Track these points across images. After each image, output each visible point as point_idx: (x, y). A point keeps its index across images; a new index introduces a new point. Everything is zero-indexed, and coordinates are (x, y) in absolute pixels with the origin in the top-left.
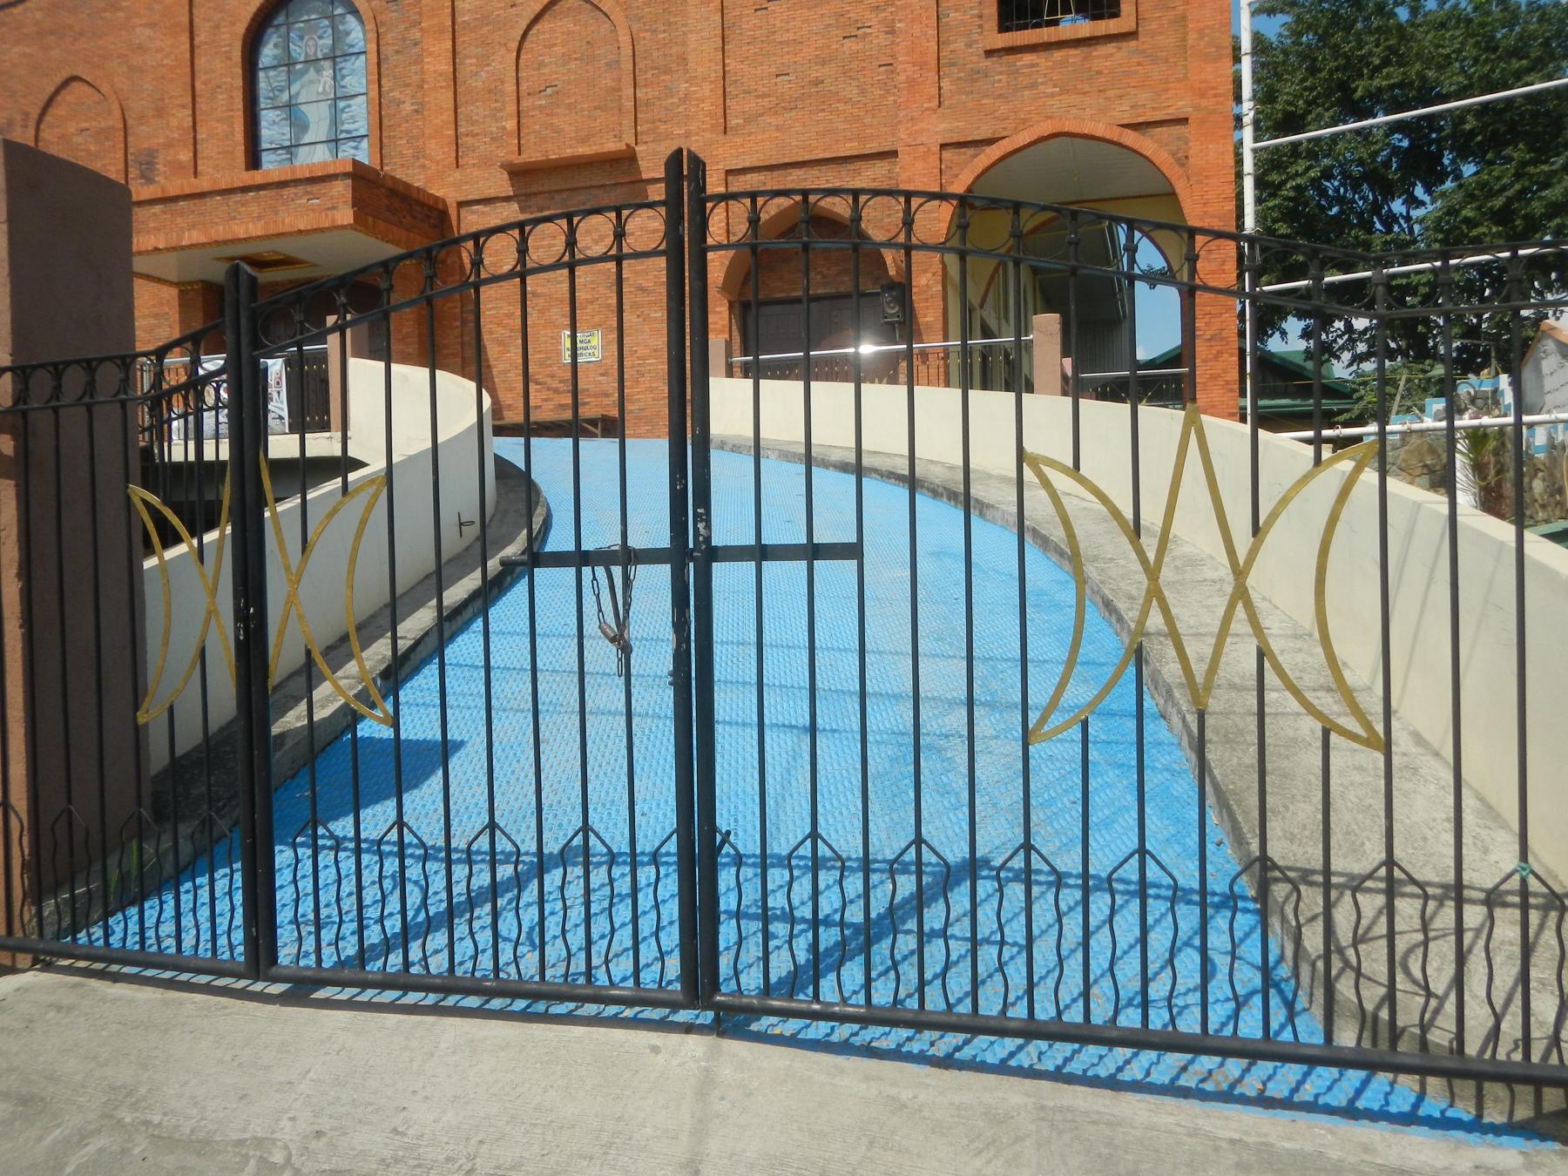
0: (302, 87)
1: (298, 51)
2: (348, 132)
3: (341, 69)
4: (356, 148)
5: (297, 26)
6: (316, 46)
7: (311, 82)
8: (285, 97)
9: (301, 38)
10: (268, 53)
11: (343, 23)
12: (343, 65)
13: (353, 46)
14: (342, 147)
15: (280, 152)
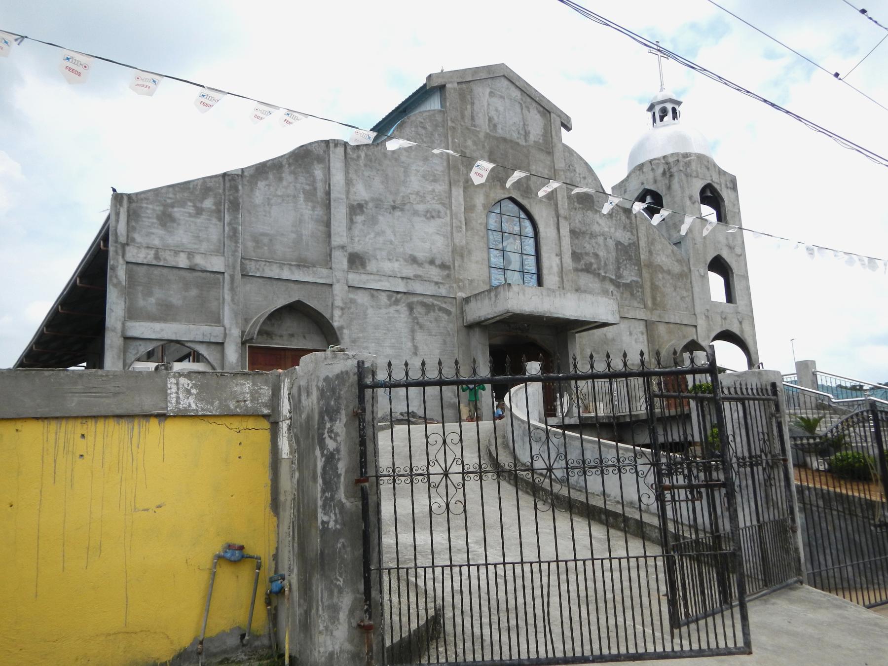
0: (508, 244)
3: (524, 242)
4: (531, 278)
6: (513, 229)
7: (512, 243)
8: (500, 247)
14: (525, 276)
15: (499, 270)
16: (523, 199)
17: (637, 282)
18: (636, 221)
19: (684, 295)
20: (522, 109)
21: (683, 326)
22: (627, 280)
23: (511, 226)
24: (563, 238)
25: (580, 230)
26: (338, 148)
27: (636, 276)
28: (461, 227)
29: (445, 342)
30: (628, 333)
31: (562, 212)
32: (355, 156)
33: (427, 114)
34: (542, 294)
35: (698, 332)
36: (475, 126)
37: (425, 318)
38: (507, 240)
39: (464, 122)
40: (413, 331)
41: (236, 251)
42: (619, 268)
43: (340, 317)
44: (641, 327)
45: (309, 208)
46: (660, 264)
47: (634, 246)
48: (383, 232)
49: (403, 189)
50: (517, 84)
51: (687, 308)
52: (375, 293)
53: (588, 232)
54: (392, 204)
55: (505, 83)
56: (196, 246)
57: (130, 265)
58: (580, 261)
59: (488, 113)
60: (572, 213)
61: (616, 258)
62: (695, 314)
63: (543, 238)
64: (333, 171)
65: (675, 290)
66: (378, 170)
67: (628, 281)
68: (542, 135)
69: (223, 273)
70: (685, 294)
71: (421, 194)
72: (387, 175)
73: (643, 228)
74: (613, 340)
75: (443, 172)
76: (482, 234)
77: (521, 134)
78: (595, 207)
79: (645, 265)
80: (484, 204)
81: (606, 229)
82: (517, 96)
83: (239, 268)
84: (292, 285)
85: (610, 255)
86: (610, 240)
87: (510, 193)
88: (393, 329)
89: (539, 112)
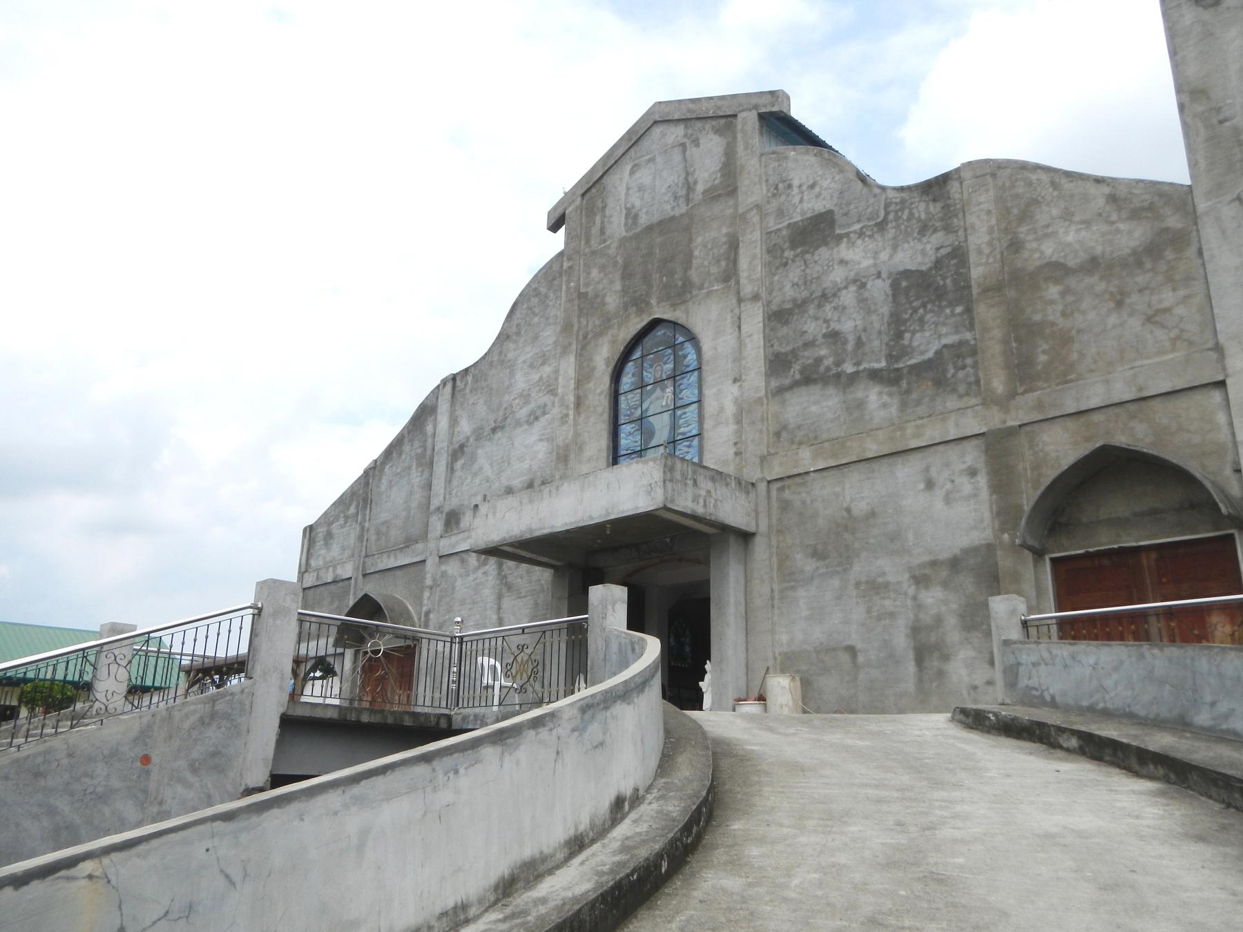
0: (651, 403)
1: (649, 377)
2: (683, 434)
3: (679, 386)
4: (689, 446)
5: (648, 357)
6: (662, 370)
7: (658, 398)
8: (638, 413)
9: (651, 366)
10: (627, 380)
11: (682, 349)
12: (681, 381)
13: (688, 366)
14: (679, 447)
15: (633, 456)
16: (674, 310)
17: (961, 344)
18: (962, 193)
19: (1166, 304)
20: (684, 152)
21: (1156, 404)
22: (922, 353)
23: (659, 368)
24: (747, 340)
25: (794, 301)
26: (446, 387)
27: (957, 332)
28: (567, 415)
29: (536, 604)
30: (922, 486)
31: (748, 289)
32: (463, 386)
33: (543, 272)
34: (521, 502)
35: (1231, 396)
36: (605, 241)
37: (515, 574)
38: (649, 397)
39: (590, 246)
40: (500, 597)
41: (361, 551)
42: (899, 335)
43: (429, 599)
44: (972, 455)
45: (419, 474)
46: (1054, 259)
47: (953, 258)
48: (481, 469)
49: (507, 398)
50: (676, 117)
51: (1173, 341)
52: (464, 555)
53: (814, 296)
54: (493, 425)
55: (657, 131)
56: (340, 557)
57: (306, 591)
58: (791, 367)
59: (626, 205)
60: (776, 278)
61: (891, 315)
62: (1218, 349)
63: (708, 362)
64: (439, 417)
65: (1120, 304)
66: (483, 389)
67: (930, 354)
68: (721, 168)
69: (351, 578)
70: (1168, 297)
71: (525, 393)
72: (491, 389)
73: (982, 199)
74: (873, 514)
75: (555, 342)
76: (600, 409)
77: (681, 196)
78: (838, 231)
79: (986, 290)
80: (608, 357)
81: (867, 263)
82: (677, 136)
83: (360, 571)
84: (398, 573)
85: (874, 318)
86: (879, 282)
87: (650, 315)
88: (479, 600)
89: (717, 131)
